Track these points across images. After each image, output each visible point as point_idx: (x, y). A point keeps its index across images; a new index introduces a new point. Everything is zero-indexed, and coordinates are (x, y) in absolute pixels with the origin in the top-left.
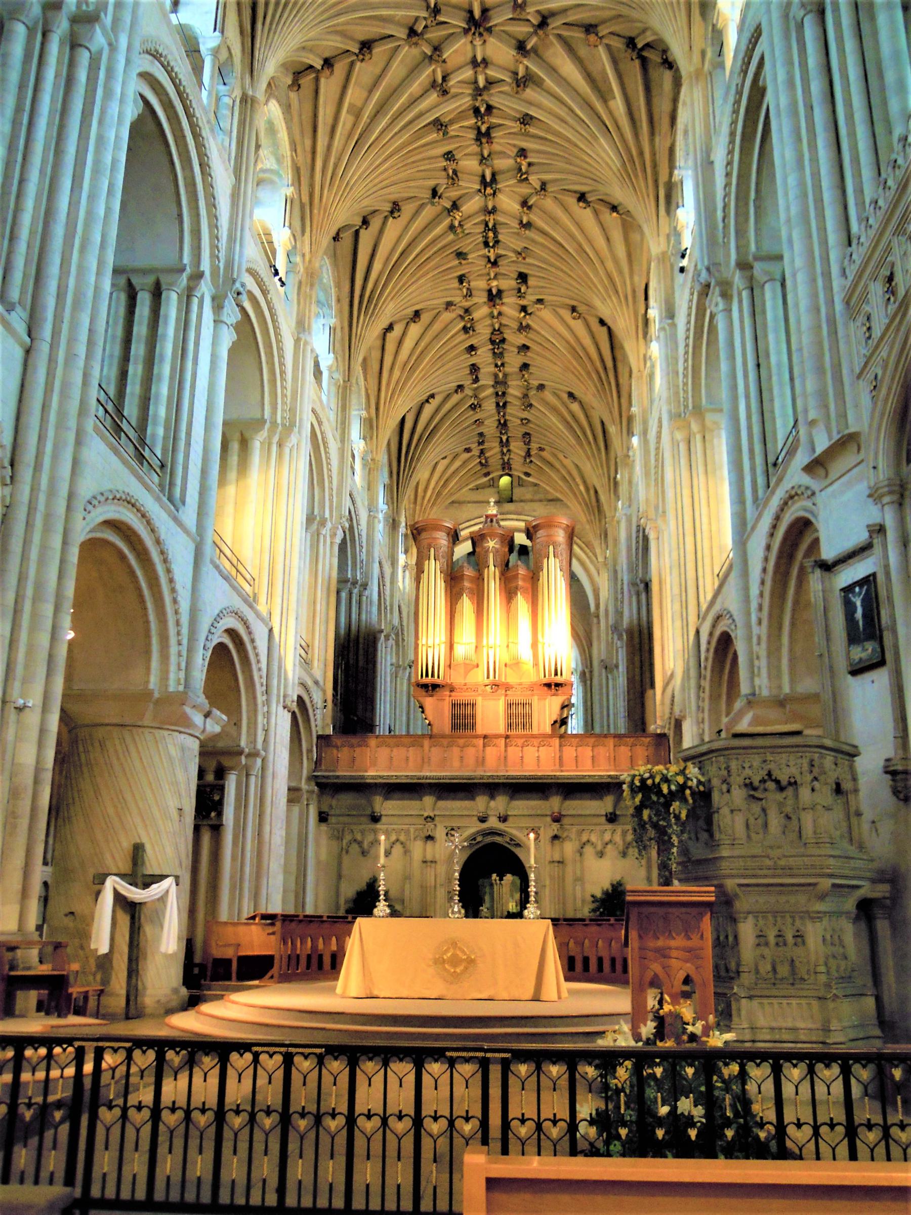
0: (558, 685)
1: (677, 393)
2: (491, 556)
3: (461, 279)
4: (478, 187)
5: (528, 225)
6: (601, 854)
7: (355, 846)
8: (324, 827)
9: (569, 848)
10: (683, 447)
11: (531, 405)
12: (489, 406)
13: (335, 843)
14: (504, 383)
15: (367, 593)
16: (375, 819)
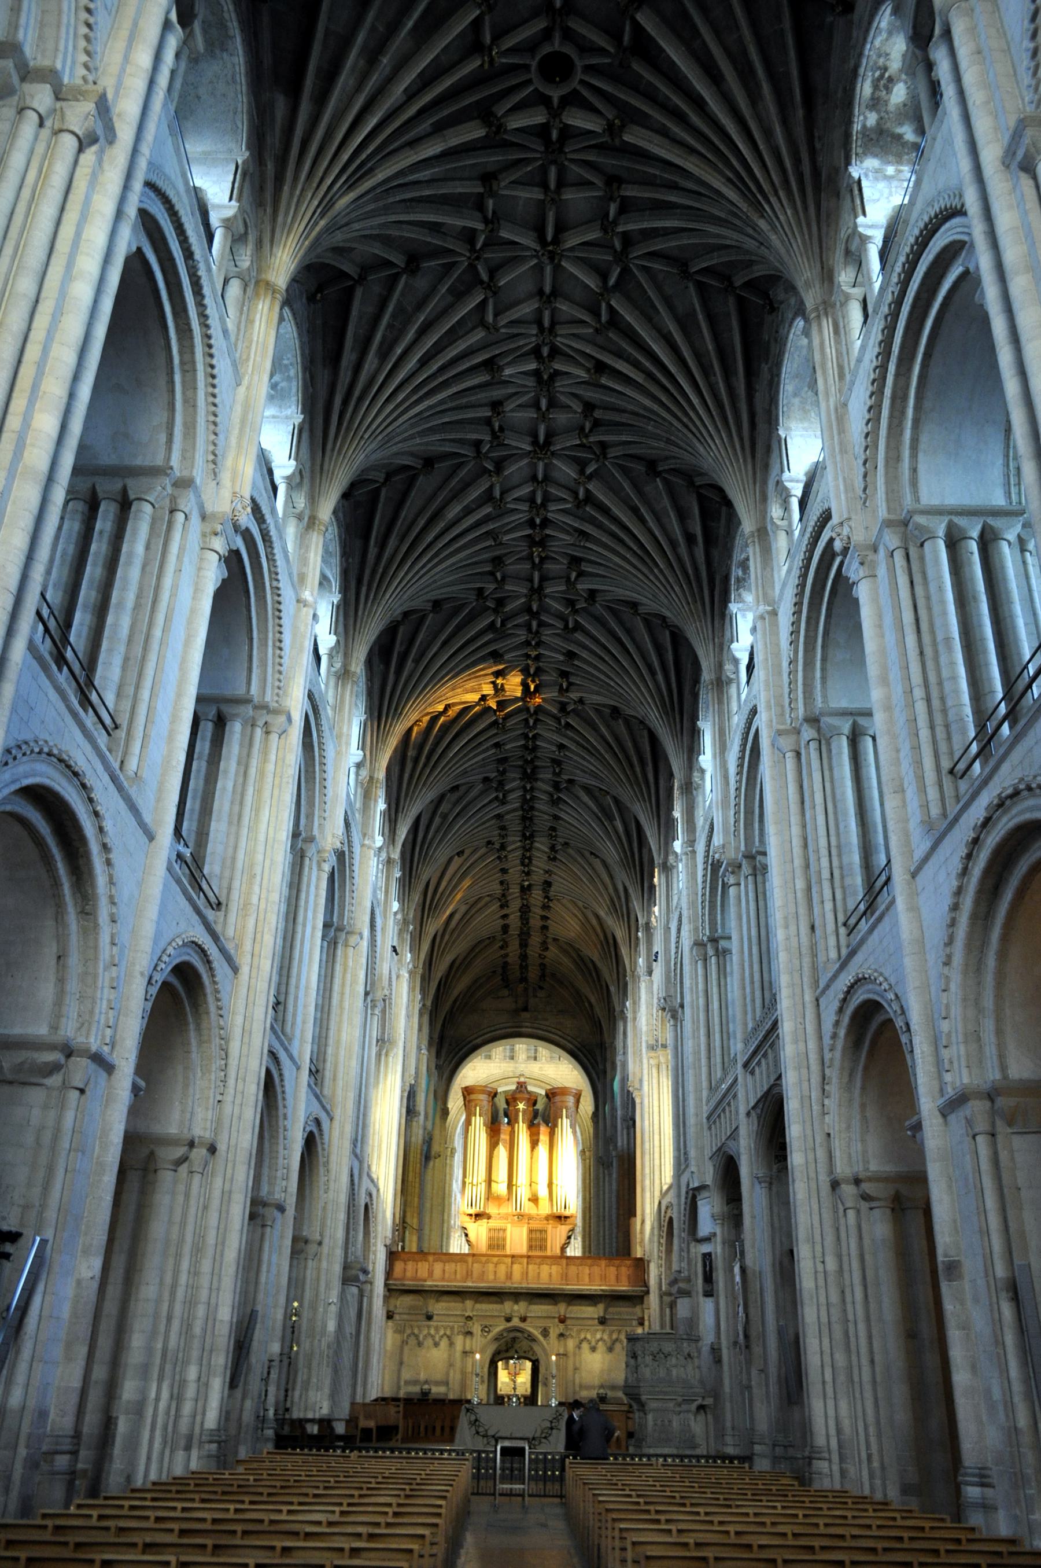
0: (566, 1217)
3: (502, 883)
5: (554, 859)
6: (593, 1349)
7: (413, 1338)
8: (390, 1323)
9: (571, 1344)
13: (398, 1336)
14: (529, 935)
16: (429, 1318)
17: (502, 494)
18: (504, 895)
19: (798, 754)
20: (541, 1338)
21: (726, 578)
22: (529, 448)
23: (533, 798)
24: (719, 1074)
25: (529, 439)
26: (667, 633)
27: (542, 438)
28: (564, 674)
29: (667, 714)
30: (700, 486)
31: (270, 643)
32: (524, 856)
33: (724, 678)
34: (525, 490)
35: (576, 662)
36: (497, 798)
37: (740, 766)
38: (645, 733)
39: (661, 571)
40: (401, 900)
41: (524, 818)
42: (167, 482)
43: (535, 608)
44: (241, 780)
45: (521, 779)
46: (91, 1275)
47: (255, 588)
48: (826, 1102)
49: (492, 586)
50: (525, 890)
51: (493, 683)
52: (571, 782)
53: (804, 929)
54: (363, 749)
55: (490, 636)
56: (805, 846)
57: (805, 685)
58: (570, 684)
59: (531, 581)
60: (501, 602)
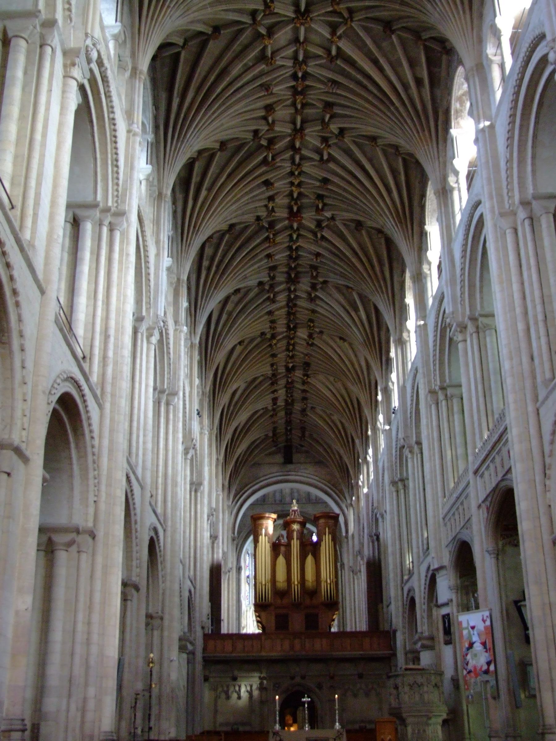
1: (392, 466)
2: (295, 533)
3: (272, 365)
4: (285, 330)
5: (313, 345)
10: (395, 494)
11: (307, 415)
12: (282, 414)
15: (216, 542)
17: (273, 53)
18: (274, 375)
19: (516, 230)
20: (317, 690)
21: (447, 112)
22: (293, 16)
23: (297, 297)
24: (452, 485)
25: (292, 8)
26: (400, 160)
27: (303, 8)
28: (320, 197)
29: (401, 222)
30: (426, 40)
31: (110, 162)
32: (289, 344)
33: (447, 188)
34: (290, 52)
35: (329, 187)
36: (268, 298)
37: (464, 251)
38: (383, 241)
39: (397, 109)
40: (200, 377)
41: (289, 314)
42: (37, 22)
43: (298, 145)
44: (94, 265)
45: (287, 283)
46: (25, 607)
47: (97, 118)
48: (548, 482)
49: (266, 128)
50: (289, 370)
51: (266, 206)
52: (325, 282)
53: (525, 359)
54: (172, 257)
55: (264, 169)
56: (524, 298)
57: (519, 177)
58: (325, 205)
59: (294, 122)
60: (271, 142)
